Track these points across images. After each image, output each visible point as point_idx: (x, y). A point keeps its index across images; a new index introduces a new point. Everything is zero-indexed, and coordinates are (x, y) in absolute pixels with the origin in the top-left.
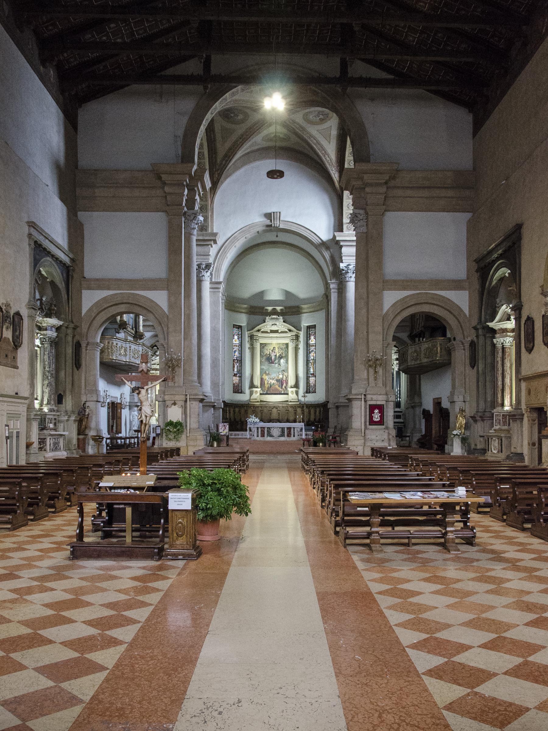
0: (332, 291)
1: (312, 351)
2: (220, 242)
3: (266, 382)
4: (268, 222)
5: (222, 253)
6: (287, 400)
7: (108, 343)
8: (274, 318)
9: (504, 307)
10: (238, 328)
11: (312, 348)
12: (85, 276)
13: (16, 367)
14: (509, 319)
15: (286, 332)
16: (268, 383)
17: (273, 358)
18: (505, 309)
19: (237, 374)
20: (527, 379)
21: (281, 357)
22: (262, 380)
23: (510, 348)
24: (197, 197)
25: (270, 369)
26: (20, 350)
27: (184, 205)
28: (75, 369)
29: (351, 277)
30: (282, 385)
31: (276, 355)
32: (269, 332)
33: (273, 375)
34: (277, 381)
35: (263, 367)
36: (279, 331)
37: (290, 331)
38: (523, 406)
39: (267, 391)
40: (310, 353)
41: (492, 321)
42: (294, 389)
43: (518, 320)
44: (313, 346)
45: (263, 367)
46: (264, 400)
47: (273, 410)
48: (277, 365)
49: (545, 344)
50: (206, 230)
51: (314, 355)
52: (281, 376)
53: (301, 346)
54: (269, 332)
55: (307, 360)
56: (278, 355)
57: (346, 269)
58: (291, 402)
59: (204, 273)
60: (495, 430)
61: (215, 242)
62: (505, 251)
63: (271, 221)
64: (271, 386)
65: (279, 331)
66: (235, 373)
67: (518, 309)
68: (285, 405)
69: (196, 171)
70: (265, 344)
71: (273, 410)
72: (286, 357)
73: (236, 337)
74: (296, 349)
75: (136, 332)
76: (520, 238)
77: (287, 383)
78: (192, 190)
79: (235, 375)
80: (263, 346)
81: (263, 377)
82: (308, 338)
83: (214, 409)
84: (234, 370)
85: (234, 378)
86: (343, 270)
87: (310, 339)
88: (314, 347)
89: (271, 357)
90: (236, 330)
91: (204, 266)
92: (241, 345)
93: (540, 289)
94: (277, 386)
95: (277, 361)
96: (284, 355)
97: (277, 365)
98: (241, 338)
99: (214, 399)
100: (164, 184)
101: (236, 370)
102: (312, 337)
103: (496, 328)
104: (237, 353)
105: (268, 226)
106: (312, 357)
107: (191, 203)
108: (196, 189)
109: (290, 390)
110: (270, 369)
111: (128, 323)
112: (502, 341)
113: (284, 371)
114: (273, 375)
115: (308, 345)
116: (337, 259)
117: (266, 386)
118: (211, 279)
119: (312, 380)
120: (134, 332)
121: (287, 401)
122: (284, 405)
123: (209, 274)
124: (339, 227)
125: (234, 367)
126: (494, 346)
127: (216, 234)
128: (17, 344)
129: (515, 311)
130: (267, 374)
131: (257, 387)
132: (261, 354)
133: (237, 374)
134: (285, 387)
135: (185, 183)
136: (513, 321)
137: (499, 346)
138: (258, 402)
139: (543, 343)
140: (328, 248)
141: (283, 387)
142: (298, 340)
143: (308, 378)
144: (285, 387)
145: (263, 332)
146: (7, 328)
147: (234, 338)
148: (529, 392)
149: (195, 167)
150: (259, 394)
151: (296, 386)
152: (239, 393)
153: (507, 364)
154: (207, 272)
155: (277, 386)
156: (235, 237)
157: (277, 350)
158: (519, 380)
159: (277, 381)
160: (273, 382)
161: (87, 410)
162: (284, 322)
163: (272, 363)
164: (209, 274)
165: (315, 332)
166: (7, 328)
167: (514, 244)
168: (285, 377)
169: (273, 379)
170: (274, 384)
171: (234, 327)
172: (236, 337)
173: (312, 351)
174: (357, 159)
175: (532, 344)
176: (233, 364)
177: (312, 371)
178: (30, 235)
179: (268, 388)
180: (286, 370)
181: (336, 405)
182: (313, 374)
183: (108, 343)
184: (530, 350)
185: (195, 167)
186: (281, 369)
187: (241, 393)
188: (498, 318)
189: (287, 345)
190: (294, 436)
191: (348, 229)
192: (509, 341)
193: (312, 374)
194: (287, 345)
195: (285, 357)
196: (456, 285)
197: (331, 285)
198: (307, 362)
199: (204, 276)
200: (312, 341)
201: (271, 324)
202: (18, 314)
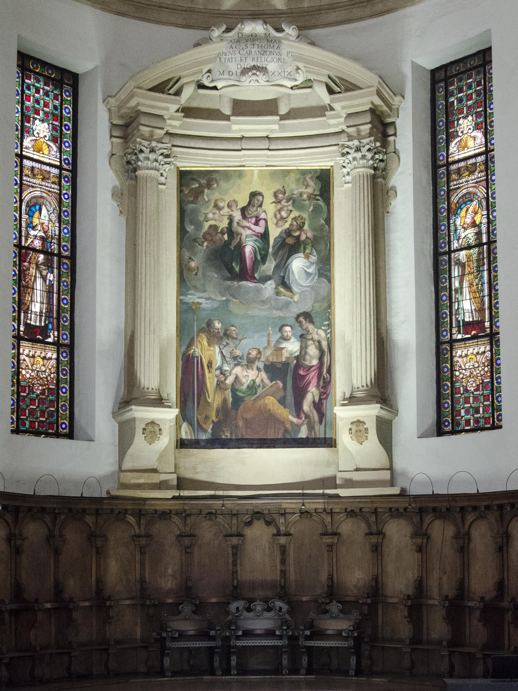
1: (468, 198)
6: (328, 472)
8: (253, 38)
10: (58, 84)
16: (220, 386)
17: (248, 250)
19: (44, 331)
25: (235, 307)
31: (265, 236)
32: (227, 111)
35: (192, 298)
36: (283, 110)
39: (217, 426)
40: (452, 212)
45: (192, 298)
46: (203, 477)
47: (249, 532)
48: (270, 285)
54: (227, 111)
55: (437, 254)
56: (274, 233)
58: (349, 484)
64: (237, 400)
65: (283, 110)
66: (34, 321)
68: (319, 504)
71: (249, 532)
81: (196, 350)
85: (26, 348)
89: (240, 247)
94: (271, 402)
96: (307, 233)
101: (36, 307)
106: (471, 233)
110: (235, 307)
113: (307, 316)
122: (311, 505)
132: (182, 231)
133: (44, 331)
134: (318, 406)
138: (162, 485)
141: (307, 405)
142: (385, 144)
144: (318, 406)
152: (57, 435)
155: (271, 402)
168: (312, 351)
169: (250, 362)
170: (252, 387)
182: (478, 324)
186: (296, 310)
187: (70, 436)
193: (467, 326)
195: (315, 242)
201: (234, 67)
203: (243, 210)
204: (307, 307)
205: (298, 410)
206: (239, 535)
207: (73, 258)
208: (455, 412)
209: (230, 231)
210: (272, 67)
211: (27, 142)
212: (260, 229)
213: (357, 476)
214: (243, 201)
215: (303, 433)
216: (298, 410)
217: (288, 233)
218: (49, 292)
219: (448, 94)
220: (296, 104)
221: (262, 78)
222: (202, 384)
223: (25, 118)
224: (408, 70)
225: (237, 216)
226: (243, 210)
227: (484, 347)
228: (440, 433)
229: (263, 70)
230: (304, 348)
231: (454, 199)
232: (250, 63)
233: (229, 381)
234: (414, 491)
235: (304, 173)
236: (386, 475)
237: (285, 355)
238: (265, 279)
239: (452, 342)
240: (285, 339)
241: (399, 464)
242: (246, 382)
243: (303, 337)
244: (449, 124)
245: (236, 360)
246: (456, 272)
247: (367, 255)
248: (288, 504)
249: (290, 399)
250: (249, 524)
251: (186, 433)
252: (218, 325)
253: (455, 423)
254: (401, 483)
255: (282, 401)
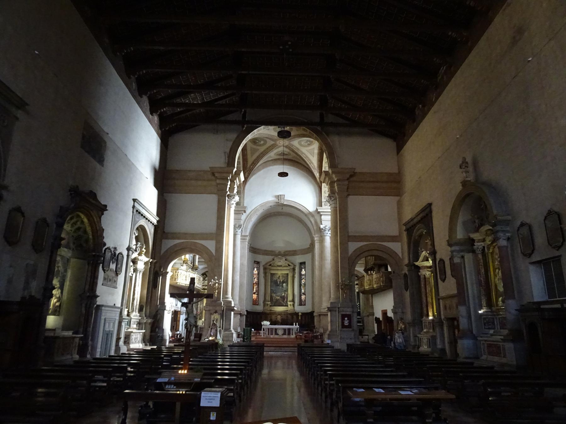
0: (316, 241)
1: (303, 278)
2: (248, 212)
3: (274, 298)
4: (277, 201)
5: (249, 218)
6: (287, 309)
7: (176, 272)
8: (279, 258)
9: (424, 252)
10: (257, 264)
11: (303, 277)
12: (165, 231)
13: (116, 288)
14: (427, 260)
15: (286, 266)
16: (275, 299)
17: (278, 283)
18: (424, 254)
19: (255, 293)
20: (443, 298)
21: (283, 282)
22: (271, 297)
23: (429, 278)
24: (236, 186)
26: (119, 276)
27: (227, 190)
28: (153, 289)
29: (327, 233)
30: (284, 300)
31: (280, 281)
32: (276, 266)
33: (279, 294)
34: (281, 297)
35: (273, 288)
37: (289, 265)
38: (443, 317)
40: (302, 280)
41: (417, 261)
42: (292, 303)
43: (434, 260)
44: (304, 275)
46: (273, 310)
47: (278, 316)
48: (281, 287)
49: (453, 276)
50: (240, 205)
51: (305, 281)
52: (283, 294)
53: (297, 276)
54: (276, 266)
57: (323, 228)
58: (289, 311)
59: (237, 230)
60: (424, 332)
61: (245, 212)
62: (422, 219)
63: (279, 201)
65: (283, 266)
67: (433, 253)
69: (236, 171)
70: (274, 274)
71: (278, 316)
72: (287, 282)
73: (255, 269)
74: (293, 277)
75: (194, 265)
76: (431, 212)
77: (287, 299)
78: (232, 181)
79: (254, 293)
80: (272, 275)
82: (301, 270)
83: (240, 316)
84: (253, 290)
85: (254, 295)
86: (323, 229)
87: (302, 271)
88: (304, 276)
90: (255, 265)
91: (237, 226)
92: (258, 274)
93: (447, 242)
94: (281, 301)
95: (281, 285)
97: (281, 287)
98: (258, 270)
99: (241, 309)
100: (216, 178)
101: (255, 290)
102: (303, 270)
103: (420, 266)
104: (256, 280)
105: (276, 203)
106: (303, 283)
107: (232, 189)
108: (235, 181)
109: (289, 303)
111: (189, 260)
112: (424, 274)
113: (285, 291)
114: (279, 294)
115: (300, 275)
116: (319, 222)
117: (274, 301)
118: (242, 233)
119: (303, 297)
120: (192, 266)
121: (287, 311)
122: (285, 314)
123: (240, 230)
124: (320, 204)
125: (254, 288)
126: (419, 277)
127: (245, 207)
128: (117, 273)
129: (431, 255)
130: (275, 293)
131: (268, 301)
134: (287, 302)
135: (229, 178)
136: (431, 262)
137: (422, 277)
138: (268, 311)
139: (451, 276)
140: (313, 216)
143: (300, 296)
144: (286, 301)
145: (272, 266)
146: (113, 263)
147: (254, 270)
148: (445, 308)
149: (235, 169)
150: (269, 306)
151: (293, 301)
152: (257, 305)
153: (428, 289)
154: (239, 229)
155: (281, 301)
156: (257, 209)
157: (281, 278)
158: (438, 300)
159: (281, 297)
160: (278, 298)
161: (159, 316)
162: (286, 260)
163: (278, 285)
164: (240, 230)
165: (305, 267)
166: (113, 263)
167: (427, 215)
168: (286, 295)
169: (278, 296)
171: (254, 263)
172: (255, 269)
173: (303, 278)
174: (331, 166)
175: (444, 276)
176: (253, 286)
177: (303, 291)
178: (134, 207)
179: (275, 302)
180: (287, 290)
181: (319, 314)
183: (176, 272)
184: (443, 280)
185: (235, 169)
186: (284, 290)
187: (258, 305)
188: (421, 259)
189: (287, 274)
190: (292, 335)
191: (325, 205)
192: (428, 273)
193: (303, 293)
194: (287, 274)
196: (393, 239)
197: (315, 238)
198: (300, 285)
199: (237, 232)
200: (303, 272)
202: (121, 253)
203: (278, 278)
204: (285, 290)
205: (284, 302)
206: (277, 317)
207: (258, 284)
208: (301, 303)
209: (276, 280)
210: (282, 261)
211: (254, 271)
212: (280, 280)
213: (291, 310)
214: (278, 277)
215: (284, 305)
216: (284, 302)
217: (283, 281)
218: (256, 288)
219: (302, 266)
220: (284, 265)
221: (280, 263)
222: (273, 299)
223: (254, 268)
224: (297, 263)
225: (277, 278)
226: (278, 278)
227: (304, 296)
228: (300, 305)
229: (280, 262)
230: (285, 294)
231: (302, 278)
232: (279, 261)
233: (276, 298)
234: (297, 312)
235: (285, 274)
236: (294, 310)
237: (282, 296)
238: (280, 286)
239: (301, 295)
240: (282, 293)
241: (296, 308)
242: (278, 298)
243: (285, 293)
244: (302, 269)
245: (277, 296)
246: (302, 287)
247: (292, 286)
248: (283, 314)
249: (283, 300)
250: (278, 315)
251: (271, 305)
252: (275, 292)
253: (302, 304)
254: (295, 311)
255: (282, 301)
